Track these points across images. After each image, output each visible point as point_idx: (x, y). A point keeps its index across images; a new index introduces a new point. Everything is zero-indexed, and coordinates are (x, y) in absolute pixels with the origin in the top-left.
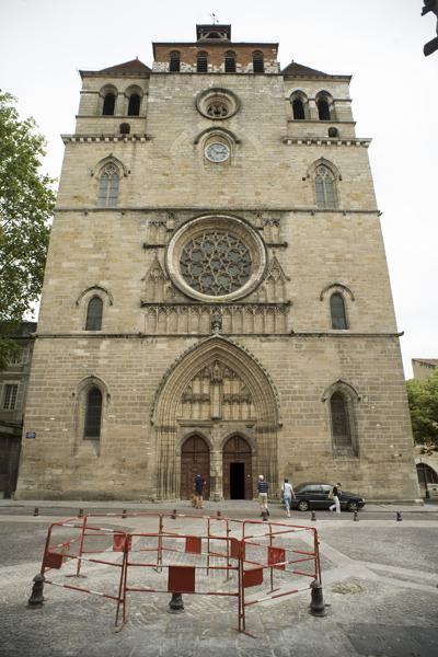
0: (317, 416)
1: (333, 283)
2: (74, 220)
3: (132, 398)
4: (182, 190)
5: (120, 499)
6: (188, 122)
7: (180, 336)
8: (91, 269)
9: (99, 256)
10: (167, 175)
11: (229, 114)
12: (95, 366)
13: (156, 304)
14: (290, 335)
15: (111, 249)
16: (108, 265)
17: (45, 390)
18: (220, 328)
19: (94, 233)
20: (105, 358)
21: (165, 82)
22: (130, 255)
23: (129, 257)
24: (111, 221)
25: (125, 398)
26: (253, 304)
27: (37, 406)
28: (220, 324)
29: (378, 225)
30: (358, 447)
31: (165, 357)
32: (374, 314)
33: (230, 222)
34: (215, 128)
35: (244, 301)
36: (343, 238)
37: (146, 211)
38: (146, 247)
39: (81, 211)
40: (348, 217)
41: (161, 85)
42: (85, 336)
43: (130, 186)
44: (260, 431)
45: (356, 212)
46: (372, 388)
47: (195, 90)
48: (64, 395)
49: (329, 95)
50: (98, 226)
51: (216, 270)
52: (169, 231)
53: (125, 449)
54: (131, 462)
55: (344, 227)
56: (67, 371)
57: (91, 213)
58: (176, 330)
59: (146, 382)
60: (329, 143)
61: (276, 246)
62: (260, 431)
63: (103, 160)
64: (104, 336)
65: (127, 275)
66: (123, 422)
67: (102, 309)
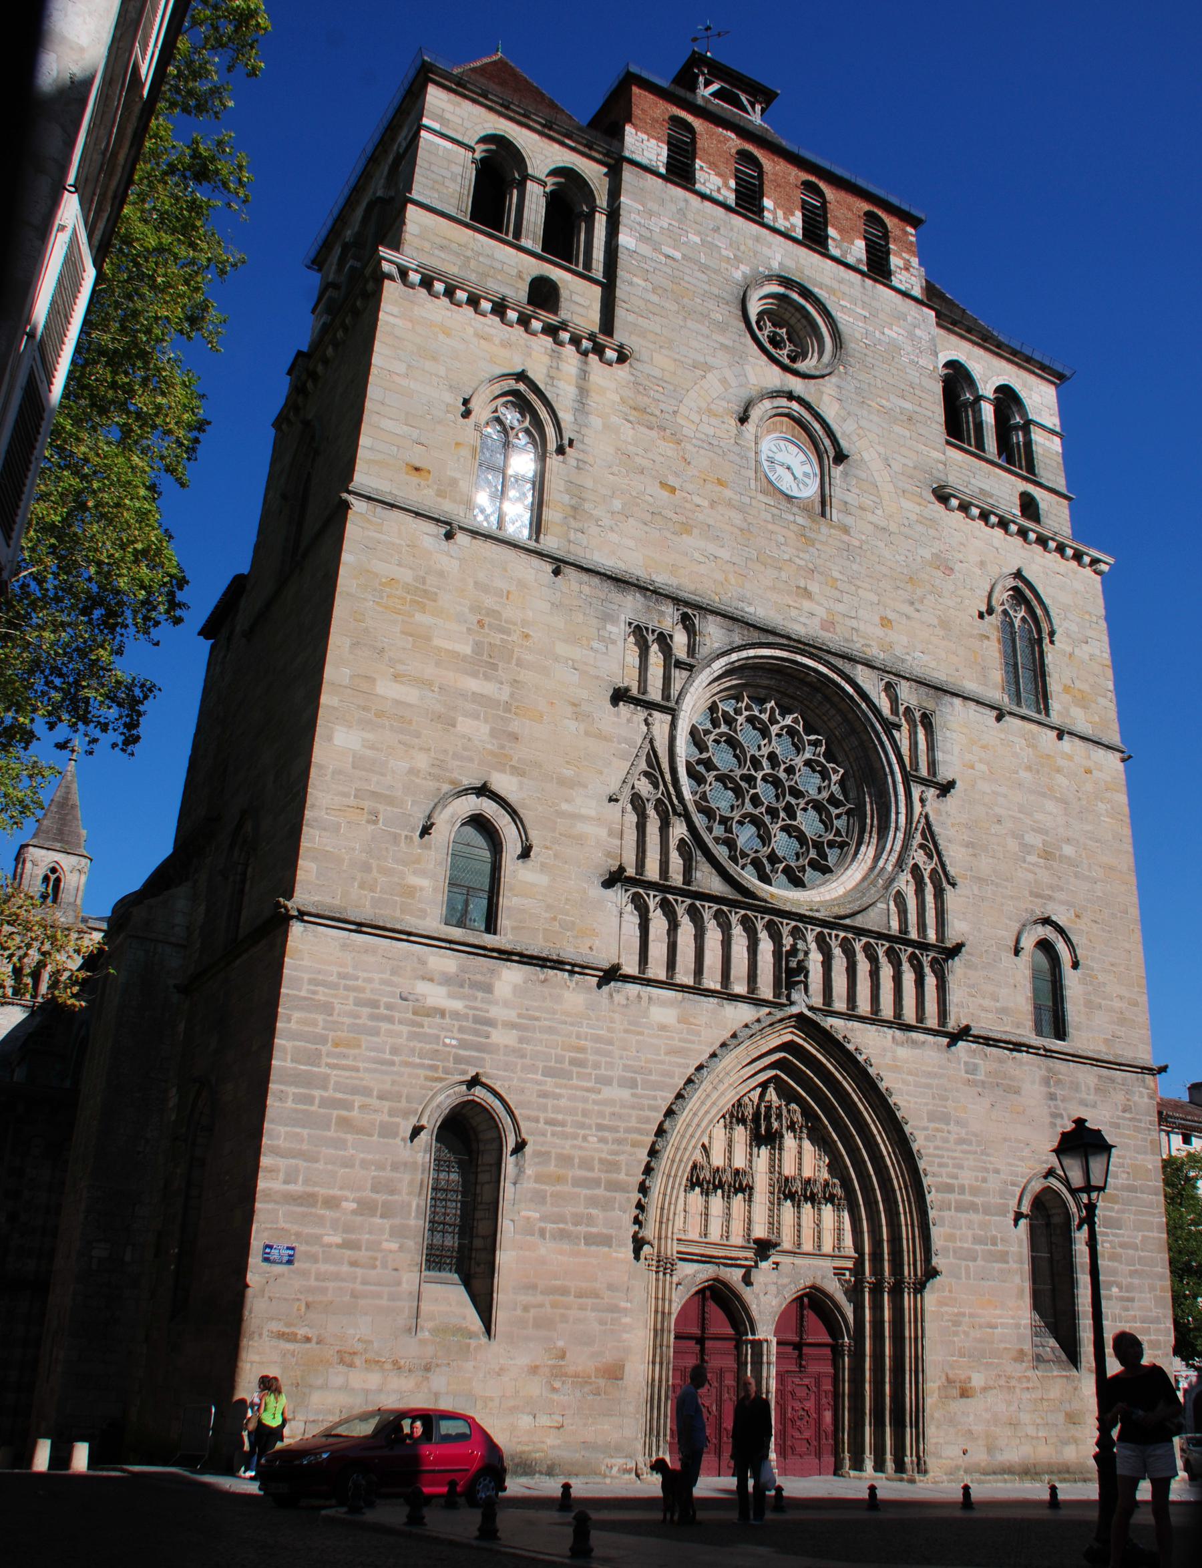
1: (1039, 914)
3: (586, 1164)
4: (712, 548)
6: (724, 347)
8: (465, 725)
10: (673, 490)
11: (801, 366)
12: (480, 1048)
15: (526, 676)
16: (515, 726)
17: (324, 1103)
19: (476, 608)
21: (662, 202)
23: (578, 716)
24: (522, 584)
25: (566, 1160)
26: (880, 936)
27: (301, 1154)
31: (671, 1052)
34: (791, 396)
35: (858, 922)
36: (1057, 800)
37: (619, 581)
40: (1067, 744)
41: (655, 207)
42: (450, 944)
45: (1083, 738)
48: (387, 1131)
50: (485, 588)
51: (773, 812)
53: (564, 1318)
55: (1058, 771)
56: (395, 1051)
57: (461, 538)
59: (620, 1117)
60: (1013, 528)
64: (505, 955)
65: (569, 772)
66: (563, 1235)
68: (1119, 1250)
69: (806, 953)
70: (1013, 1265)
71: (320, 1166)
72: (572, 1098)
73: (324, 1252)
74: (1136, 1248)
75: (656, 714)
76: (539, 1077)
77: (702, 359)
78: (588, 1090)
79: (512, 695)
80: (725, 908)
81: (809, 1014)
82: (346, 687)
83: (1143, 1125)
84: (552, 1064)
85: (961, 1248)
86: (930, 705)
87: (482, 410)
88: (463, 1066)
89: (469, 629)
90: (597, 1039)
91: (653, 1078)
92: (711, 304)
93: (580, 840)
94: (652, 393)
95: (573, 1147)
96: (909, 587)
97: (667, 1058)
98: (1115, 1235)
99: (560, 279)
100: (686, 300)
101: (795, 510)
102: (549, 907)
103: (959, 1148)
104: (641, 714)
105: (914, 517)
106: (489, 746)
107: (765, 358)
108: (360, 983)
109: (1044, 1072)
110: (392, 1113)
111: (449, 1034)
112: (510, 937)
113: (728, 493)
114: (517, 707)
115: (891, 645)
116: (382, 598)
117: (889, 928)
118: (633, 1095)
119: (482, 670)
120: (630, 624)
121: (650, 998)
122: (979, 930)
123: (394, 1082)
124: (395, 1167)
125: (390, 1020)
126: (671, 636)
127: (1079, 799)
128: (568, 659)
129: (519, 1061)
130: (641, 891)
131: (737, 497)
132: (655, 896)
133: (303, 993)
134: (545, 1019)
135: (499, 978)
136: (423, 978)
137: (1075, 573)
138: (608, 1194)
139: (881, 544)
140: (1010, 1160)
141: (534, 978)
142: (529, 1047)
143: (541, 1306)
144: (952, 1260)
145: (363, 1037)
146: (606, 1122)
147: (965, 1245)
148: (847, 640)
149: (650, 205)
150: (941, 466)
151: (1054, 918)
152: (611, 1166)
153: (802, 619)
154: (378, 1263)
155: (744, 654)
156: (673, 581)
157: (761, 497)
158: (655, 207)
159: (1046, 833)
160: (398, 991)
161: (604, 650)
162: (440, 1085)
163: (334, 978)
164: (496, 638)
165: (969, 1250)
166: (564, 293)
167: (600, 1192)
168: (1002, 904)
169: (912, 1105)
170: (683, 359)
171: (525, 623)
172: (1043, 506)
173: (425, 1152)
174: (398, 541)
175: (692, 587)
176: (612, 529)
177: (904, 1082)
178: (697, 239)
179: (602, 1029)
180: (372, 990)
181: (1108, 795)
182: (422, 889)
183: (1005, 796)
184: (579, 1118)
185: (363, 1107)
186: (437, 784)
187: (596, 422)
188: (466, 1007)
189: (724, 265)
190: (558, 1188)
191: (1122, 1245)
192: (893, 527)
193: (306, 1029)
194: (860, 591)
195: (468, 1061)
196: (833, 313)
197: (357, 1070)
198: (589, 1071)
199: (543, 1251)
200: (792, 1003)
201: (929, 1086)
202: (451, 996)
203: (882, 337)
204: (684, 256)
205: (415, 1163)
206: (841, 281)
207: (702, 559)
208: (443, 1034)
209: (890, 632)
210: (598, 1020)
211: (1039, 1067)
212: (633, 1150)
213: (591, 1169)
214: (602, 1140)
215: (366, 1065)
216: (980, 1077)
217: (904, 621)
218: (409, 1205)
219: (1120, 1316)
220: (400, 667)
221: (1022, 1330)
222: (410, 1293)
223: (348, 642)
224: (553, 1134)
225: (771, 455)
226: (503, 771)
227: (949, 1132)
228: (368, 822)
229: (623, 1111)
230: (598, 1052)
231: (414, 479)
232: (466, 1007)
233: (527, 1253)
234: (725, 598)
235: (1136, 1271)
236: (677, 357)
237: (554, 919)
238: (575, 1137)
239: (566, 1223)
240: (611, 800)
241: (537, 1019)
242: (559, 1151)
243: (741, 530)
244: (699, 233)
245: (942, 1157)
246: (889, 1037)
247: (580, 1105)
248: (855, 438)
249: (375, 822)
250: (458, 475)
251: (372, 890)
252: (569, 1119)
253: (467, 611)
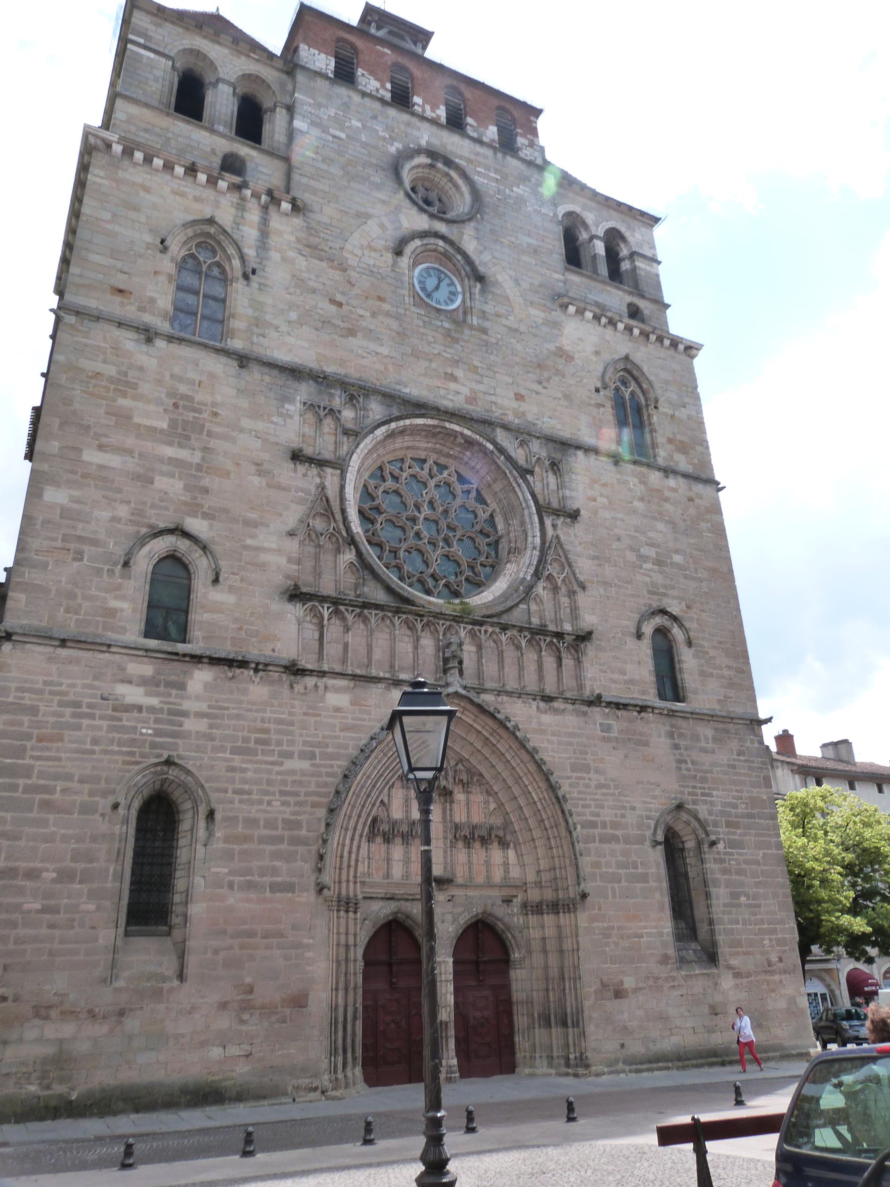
0: (644, 878)
1: (655, 605)
2: (117, 349)
3: (270, 824)
4: (373, 346)
5: (241, 1096)
7: (377, 680)
9: (183, 454)
10: (340, 305)
12: (174, 735)
13: (323, 599)
14: (590, 703)
15: (214, 443)
16: (206, 482)
17: (27, 789)
18: (461, 673)
19: (172, 394)
20: (201, 715)
21: (329, 97)
22: (260, 469)
23: (260, 473)
24: (212, 376)
25: (252, 823)
26: (521, 629)
28: (461, 663)
29: (716, 509)
30: (714, 944)
31: (346, 728)
32: (722, 677)
33: (470, 443)
34: (437, 235)
35: (504, 619)
36: (667, 522)
37: (294, 372)
38: (297, 456)
39: (137, 329)
40: (672, 482)
43: (256, 305)
44: (538, 909)
46: (728, 824)
47: (392, 139)
48: (87, 809)
49: (623, 238)
50: (180, 379)
52: (346, 432)
54: (267, 993)
55: (667, 500)
56: (95, 741)
57: (160, 343)
58: (369, 665)
59: (301, 783)
61: (557, 513)
62: (538, 909)
63: (195, 222)
64: (197, 659)
65: (253, 516)
66: (249, 886)
67: (189, 590)
68: (744, 866)
69: (460, 645)
71: (23, 843)
72: (257, 771)
73: (23, 918)
74: (757, 863)
75: (329, 471)
76: (228, 755)
77: (363, 210)
78: (272, 763)
79: (203, 459)
80: (390, 614)
81: (464, 692)
82: (54, 456)
83: (756, 765)
84: (239, 744)
85: (606, 873)
86: (558, 456)
87: (176, 249)
88: (158, 751)
89: (165, 410)
90: (280, 722)
91: (330, 750)
92: (371, 171)
93: (263, 566)
94: (322, 235)
95: (259, 811)
96: (538, 371)
97: (342, 734)
98: (739, 854)
99: (248, 155)
100: (350, 168)
101: (442, 317)
102: (236, 620)
103: (599, 791)
104: (314, 471)
105: (541, 321)
106: (183, 498)
107: (415, 208)
108: (63, 688)
109: (668, 728)
110: (91, 793)
111: (146, 725)
112: (201, 644)
113: (386, 307)
114: (208, 468)
115: (524, 414)
116: (89, 388)
117: (530, 623)
118: (312, 765)
119: (176, 440)
120: (305, 404)
121: (326, 688)
122: (607, 621)
123: (93, 768)
124: (94, 839)
125: (92, 716)
126: (339, 412)
127: (684, 520)
128: (251, 431)
129: (210, 743)
130: (317, 604)
131: (395, 309)
132: (328, 608)
133: (10, 699)
134: (233, 709)
135: (192, 678)
136: (123, 681)
137: (673, 357)
138: (292, 848)
139: (514, 341)
140: (646, 799)
141: (223, 676)
142: (219, 732)
143: (230, 948)
144: (599, 883)
145: (66, 732)
146: (288, 789)
147: (610, 870)
148: (487, 411)
149: (320, 99)
150: (561, 284)
151: (669, 610)
152: (293, 825)
153: (450, 397)
154: (76, 924)
155: (401, 423)
156: (342, 371)
157: (413, 309)
158: (324, 101)
159: (659, 547)
160: (99, 693)
161: (283, 423)
162: (136, 768)
163: (40, 686)
164: (190, 416)
165: (613, 874)
166: (250, 165)
167: (284, 846)
168: (624, 601)
169: (557, 760)
170: (347, 210)
171: (214, 404)
172: (646, 312)
173: (123, 823)
174: (103, 345)
175: (357, 375)
176: (289, 334)
177: (549, 741)
178: (359, 125)
179: (284, 713)
180: (75, 693)
181: (708, 516)
182: (122, 610)
183: (623, 520)
184: (264, 787)
185: (64, 791)
186: (136, 528)
187: (275, 256)
188: (162, 702)
189: (381, 143)
190: (245, 846)
192: (523, 328)
193: (12, 728)
194: (497, 375)
195: (162, 746)
196: (472, 177)
197: (59, 759)
198: (272, 748)
199: (231, 901)
200: (447, 685)
201: (570, 744)
202: (148, 694)
203: (512, 194)
204: (348, 136)
205: (113, 834)
206: (478, 154)
207: (365, 355)
208: (140, 725)
209: (523, 404)
210: (280, 706)
211: (664, 724)
212: (313, 810)
213: (276, 829)
214: (284, 804)
215: (68, 755)
216: (615, 734)
217: (534, 395)
218: (107, 870)
220: (104, 440)
221: (665, 937)
222: (106, 947)
223: (57, 422)
224: (240, 802)
225: (423, 279)
226: (196, 516)
227: (590, 779)
228: (74, 559)
229: (303, 778)
230: (279, 732)
231: (118, 299)
232: (162, 702)
233: (216, 904)
234: (385, 383)
235: (760, 882)
236: (343, 208)
237: (241, 629)
238: (260, 802)
239: (253, 875)
240: (291, 535)
241: (227, 709)
242: (246, 815)
243: (398, 333)
244: (360, 120)
245: (585, 799)
246: (534, 707)
247: (265, 776)
248: (490, 265)
249: (81, 560)
250: (156, 295)
251: (77, 613)
252: (255, 788)
253: (163, 396)
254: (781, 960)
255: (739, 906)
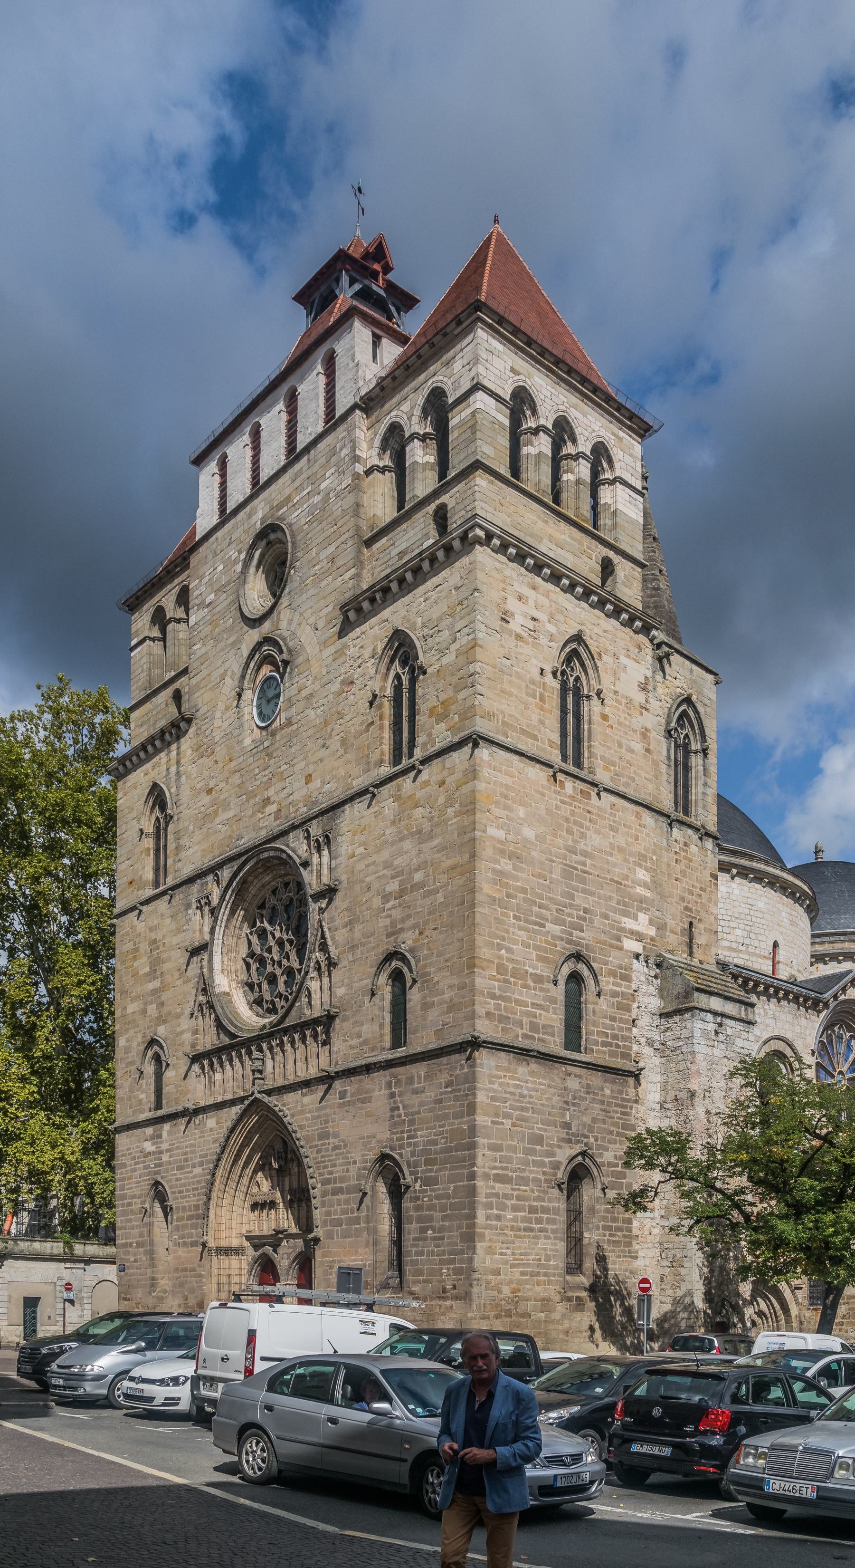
46: (428, 1162)
70: (363, 1225)
74: (448, 1197)
191: (437, 1197)
219: (433, 1251)
235: (447, 1216)
254: (454, 1287)
255: (425, 1239)
